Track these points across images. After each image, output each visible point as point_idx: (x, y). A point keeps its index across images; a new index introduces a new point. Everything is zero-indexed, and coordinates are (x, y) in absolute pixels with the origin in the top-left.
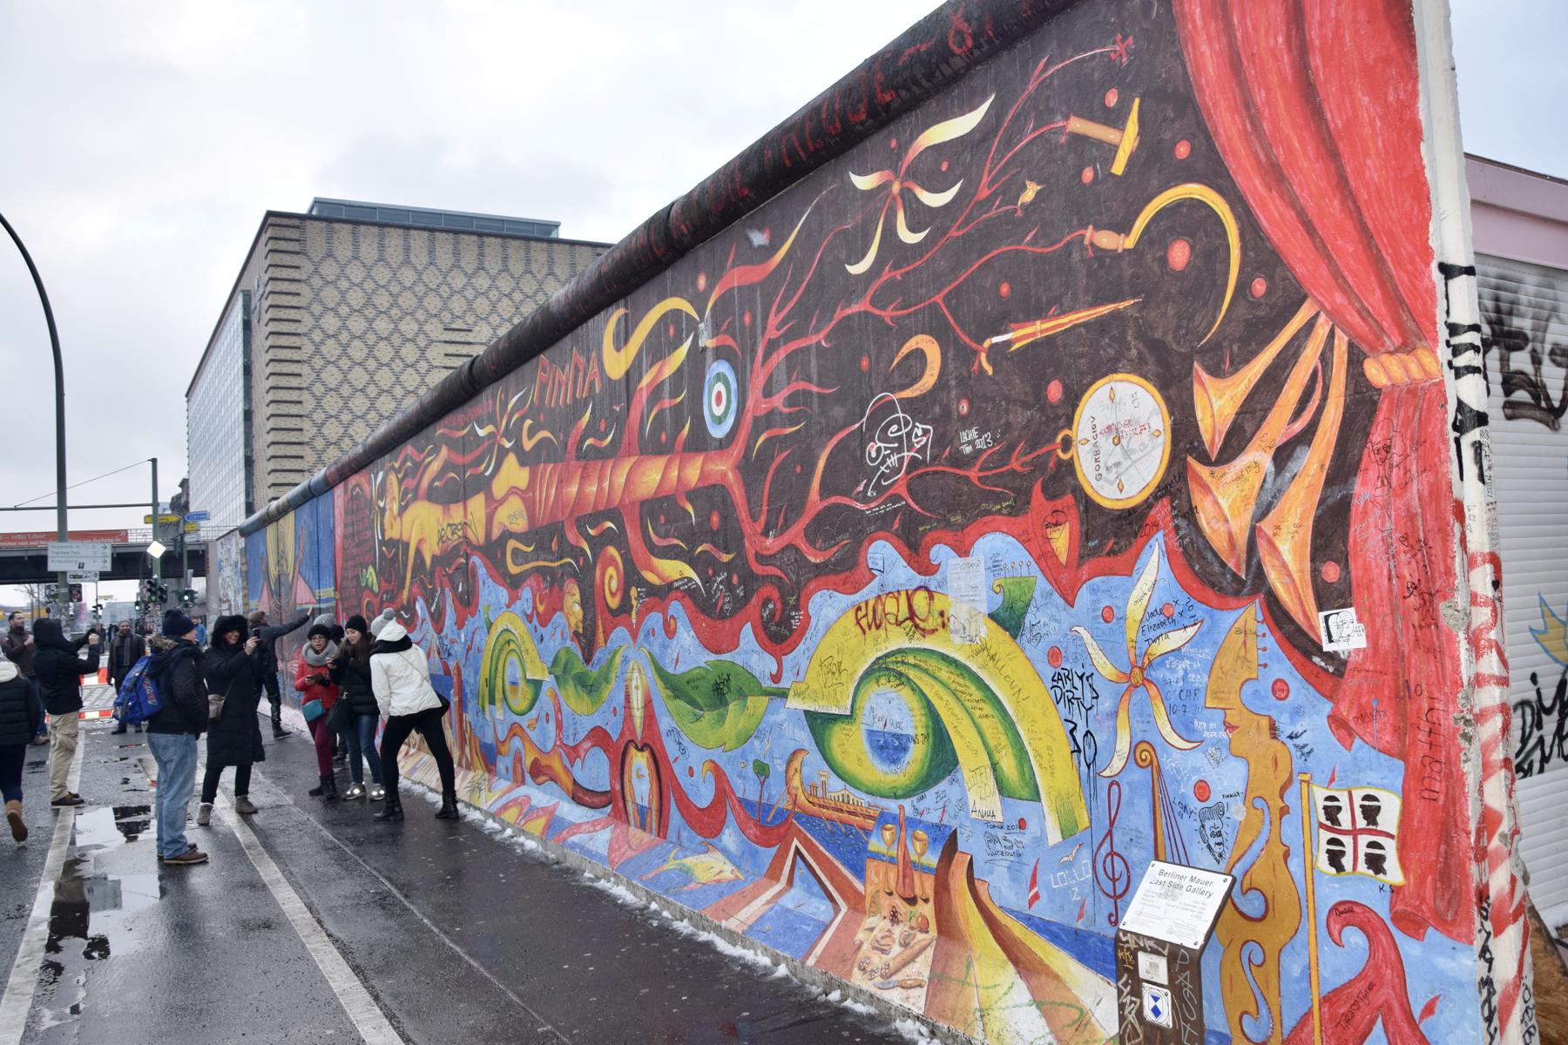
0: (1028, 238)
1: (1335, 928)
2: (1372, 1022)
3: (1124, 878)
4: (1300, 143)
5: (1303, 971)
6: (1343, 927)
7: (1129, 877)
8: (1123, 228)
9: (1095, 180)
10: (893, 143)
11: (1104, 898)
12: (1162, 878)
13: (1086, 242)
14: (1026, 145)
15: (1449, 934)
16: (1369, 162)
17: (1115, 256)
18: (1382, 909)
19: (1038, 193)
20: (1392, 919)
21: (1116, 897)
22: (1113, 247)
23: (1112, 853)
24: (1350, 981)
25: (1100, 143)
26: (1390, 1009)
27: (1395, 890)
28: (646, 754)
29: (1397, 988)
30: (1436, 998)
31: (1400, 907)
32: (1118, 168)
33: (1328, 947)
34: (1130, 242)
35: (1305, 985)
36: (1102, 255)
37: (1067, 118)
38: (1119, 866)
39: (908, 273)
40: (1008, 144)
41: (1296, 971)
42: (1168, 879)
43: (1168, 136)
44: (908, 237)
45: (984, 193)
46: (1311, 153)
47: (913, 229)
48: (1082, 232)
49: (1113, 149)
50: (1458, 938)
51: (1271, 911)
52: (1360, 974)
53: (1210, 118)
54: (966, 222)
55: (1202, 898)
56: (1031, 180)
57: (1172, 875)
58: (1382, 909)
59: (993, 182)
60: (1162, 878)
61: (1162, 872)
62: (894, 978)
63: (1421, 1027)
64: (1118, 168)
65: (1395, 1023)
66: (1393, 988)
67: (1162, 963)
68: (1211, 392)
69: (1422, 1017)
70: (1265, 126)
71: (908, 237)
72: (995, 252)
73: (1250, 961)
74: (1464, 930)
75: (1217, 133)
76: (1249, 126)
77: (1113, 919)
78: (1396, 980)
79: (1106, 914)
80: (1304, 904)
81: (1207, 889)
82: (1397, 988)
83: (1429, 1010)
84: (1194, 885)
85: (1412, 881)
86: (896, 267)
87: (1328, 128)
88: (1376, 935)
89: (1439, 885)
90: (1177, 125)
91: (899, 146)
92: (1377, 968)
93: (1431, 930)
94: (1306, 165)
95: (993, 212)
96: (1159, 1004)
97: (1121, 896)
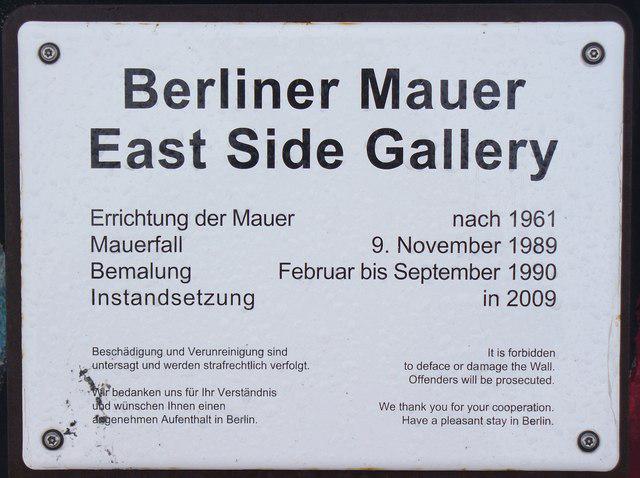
12: (159, 123)
42: (216, 122)
57: (231, 87)
60: (159, 123)
84: (416, 125)
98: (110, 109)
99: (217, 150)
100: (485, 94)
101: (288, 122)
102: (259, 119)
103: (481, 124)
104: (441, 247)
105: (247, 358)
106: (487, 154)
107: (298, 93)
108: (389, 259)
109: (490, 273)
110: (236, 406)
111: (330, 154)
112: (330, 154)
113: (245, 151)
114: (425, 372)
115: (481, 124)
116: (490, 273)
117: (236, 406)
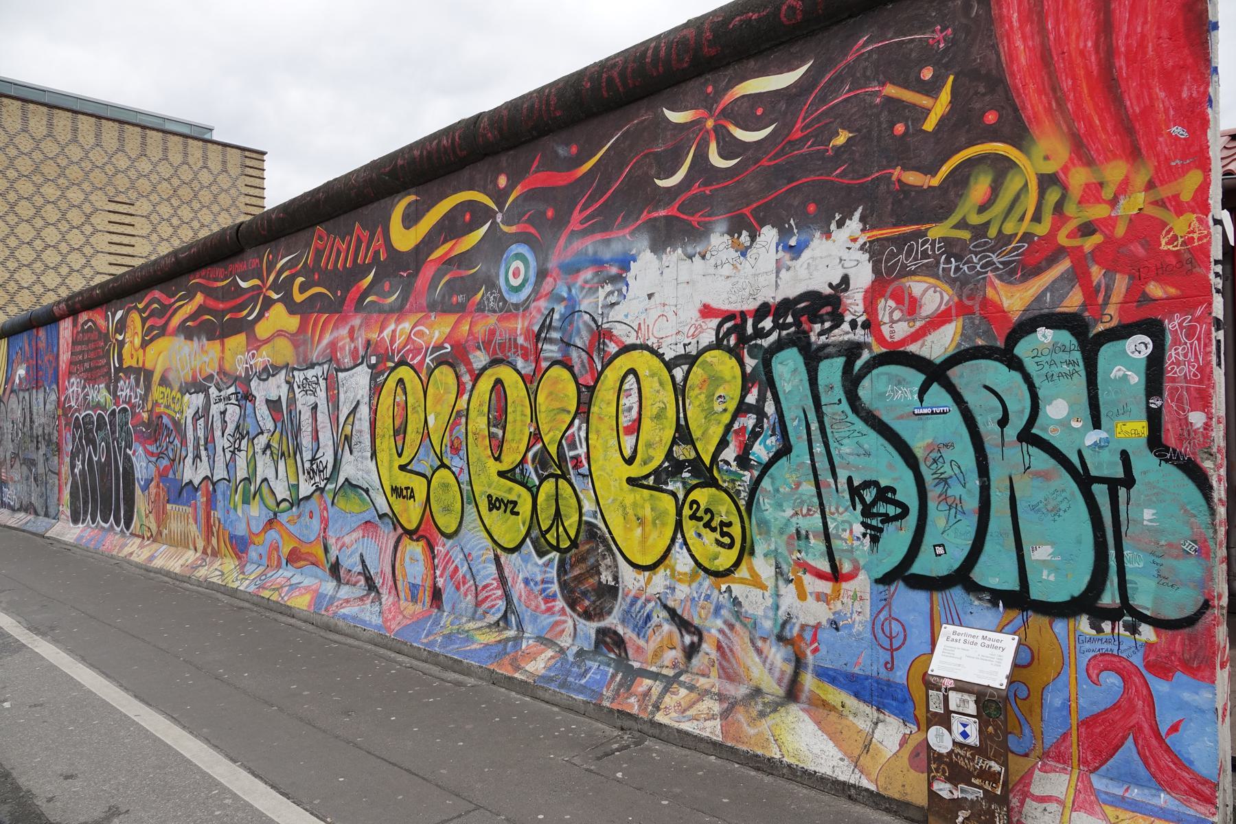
0: (838, 172)
1: (1094, 674)
2: (1124, 738)
3: (902, 636)
4: (1100, 120)
5: (1063, 704)
6: (1101, 671)
7: (905, 636)
8: (932, 171)
9: (906, 133)
10: (710, 89)
11: (881, 650)
12: (956, 637)
13: (894, 178)
14: (841, 102)
15: (1195, 676)
16: (1161, 139)
17: (919, 190)
18: (1137, 660)
19: (849, 139)
20: (1145, 666)
21: (892, 650)
22: (919, 184)
23: (891, 618)
24: (1106, 710)
25: (914, 106)
26: (1141, 729)
27: (1149, 645)
28: (422, 543)
29: (1147, 714)
30: (1181, 721)
31: (1152, 658)
32: (930, 125)
33: (1086, 685)
34: (935, 182)
35: (1065, 713)
36: (905, 189)
37: (883, 84)
38: (896, 627)
39: (716, 190)
40: (823, 99)
41: (1058, 702)
42: (963, 638)
43: (978, 106)
44: (716, 161)
45: (797, 134)
46: (1109, 127)
47: (724, 156)
48: (891, 171)
49: (926, 112)
50: (1203, 679)
51: (1036, 660)
52: (1115, 705)
53: (1019, 95)
54: (777, 156)
55: (998, 652)
56: (844, 129)
58: (1137, 660)
59: (806, 127)
60: (956, 637)
61: (954, 633)
62: (688, 713)
63: (1167, 741)
64: (930, 125)
65: (1145, 739)
66: (1144, 714)
67: (971, 699)
68: (1002, 293)
69: (1168, 734)
70: (1069, 106)
71: (716, 161)
72: (804, 180)
73: (1015, 695)
74: (1207, 674)
75: (1024, 108)
76: (1054, 104)
77: (889, 666)
78: (1147, 709)
79: (882, 662)
80: (1066, 653)
81: (999, 645)
82: (1147, 714)
83: (1174, 728)
84: (987, 642)
85: (1164, 639)
86: (706, 184)
87: (1126, 111)
88: (1130, 677)
89: (1187, 642)
90: (987, 98)
91: (716, 92)
92: (1130, 700)
93: (1178, 674)
94: (1104, 137)
95: (805, 149)
96: (968, 729)
97: (897, 649)
99: (962, 641)
100: (998, 641)
101: (972, 639)
102: (968, 638)
103: (996, 644)
106: (996, 648)
107: (974, 637)
111: (976, 644)
112: (976, 644)
113: (965, 641)
114: (981, 671)
115: (996, 644)
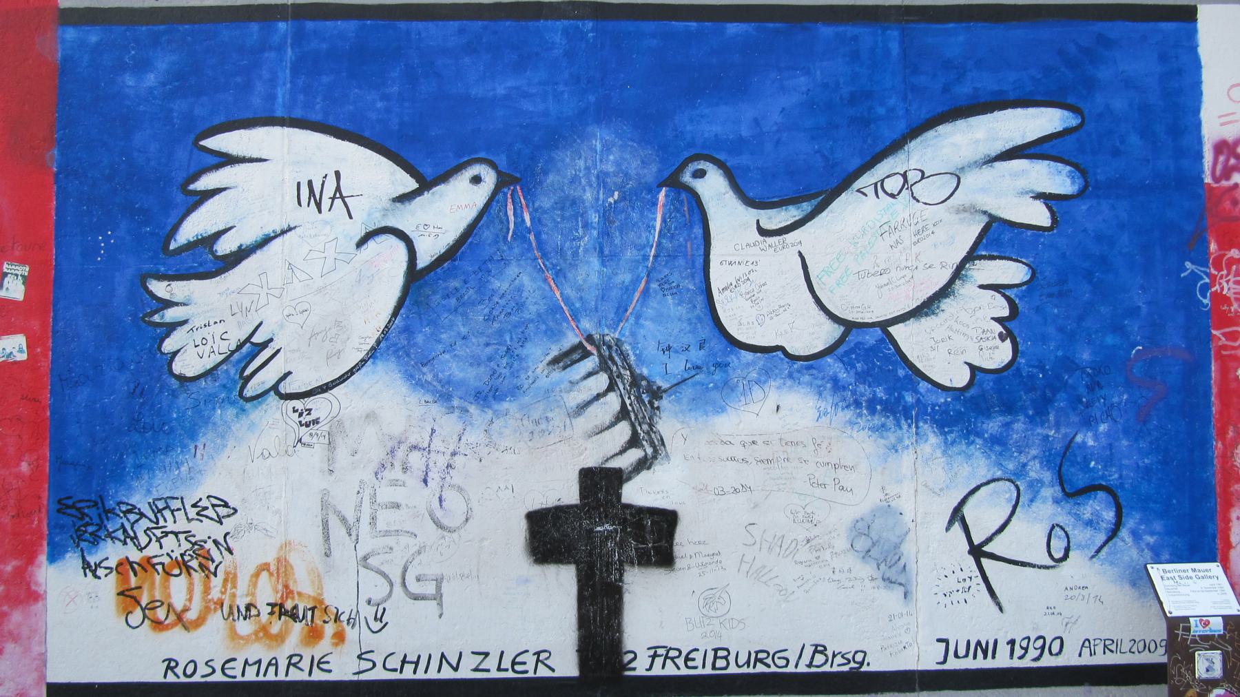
42: (1176, 575)
60: (1168, 575)
98: (1163, 574)
101: (1185, 575)
103: (1209, 574)
104: (1210, 588)
105: (1189, 602)
108: (1204, 589)
109: (1217, 591)
110: (1193, 607)
111: (1191, 578)
112: (1191, 578)
114: (1215, 603)
116: (1217, 591)
117: (1193, 607)
